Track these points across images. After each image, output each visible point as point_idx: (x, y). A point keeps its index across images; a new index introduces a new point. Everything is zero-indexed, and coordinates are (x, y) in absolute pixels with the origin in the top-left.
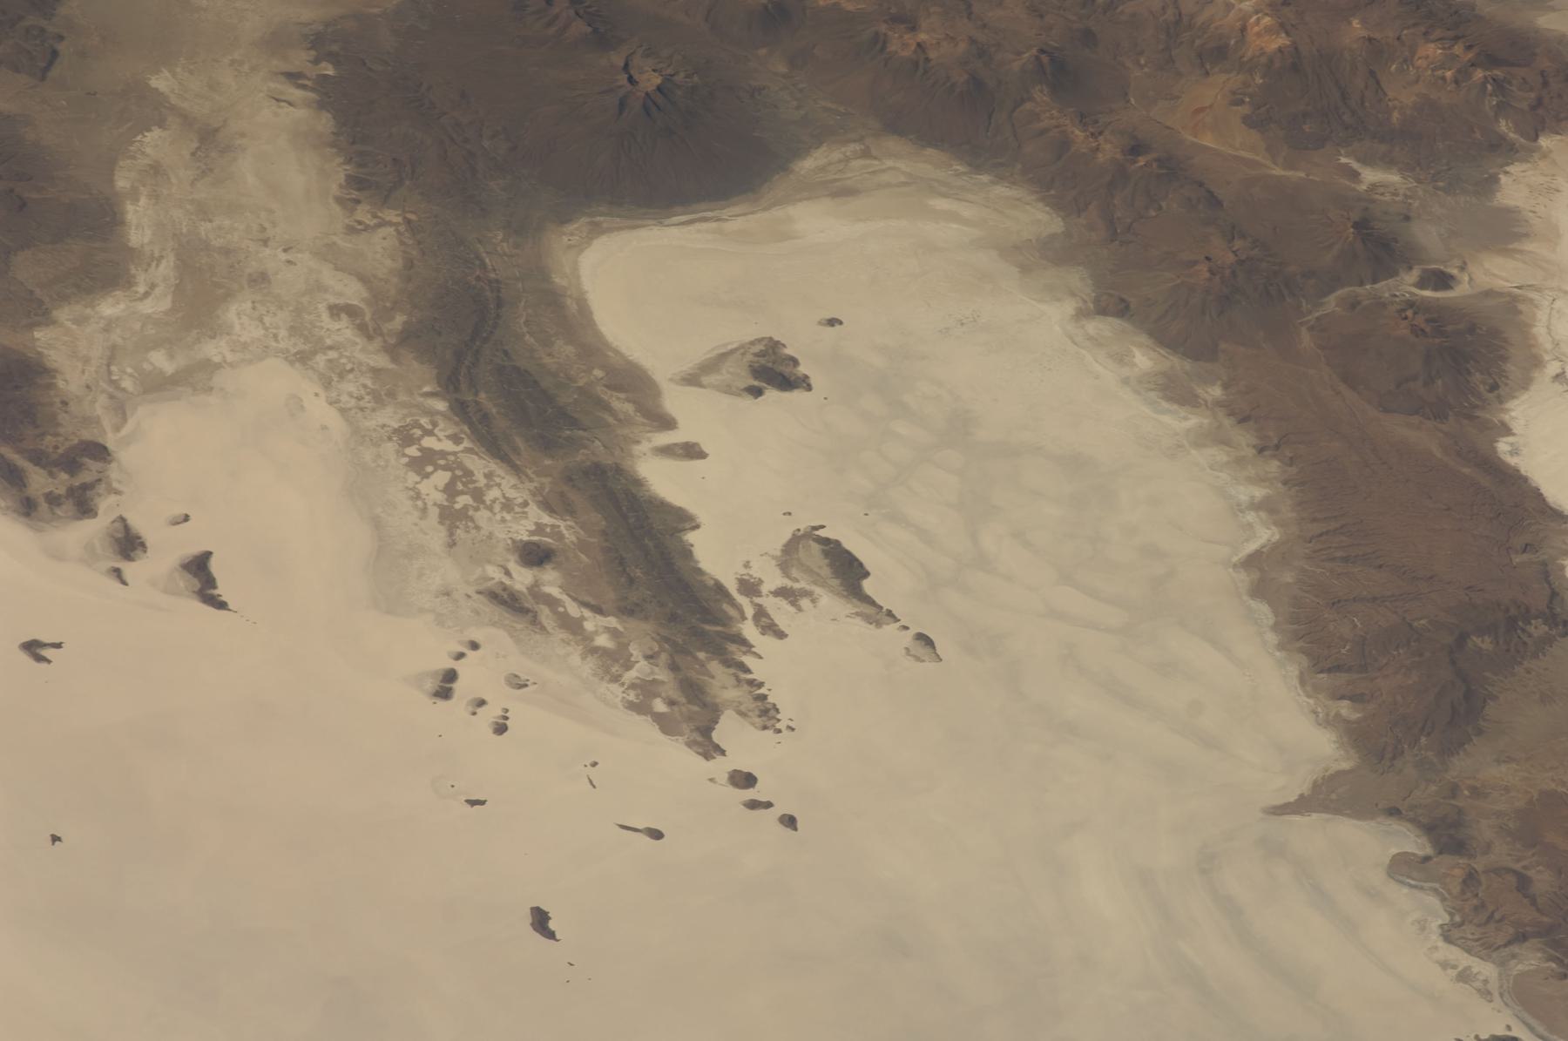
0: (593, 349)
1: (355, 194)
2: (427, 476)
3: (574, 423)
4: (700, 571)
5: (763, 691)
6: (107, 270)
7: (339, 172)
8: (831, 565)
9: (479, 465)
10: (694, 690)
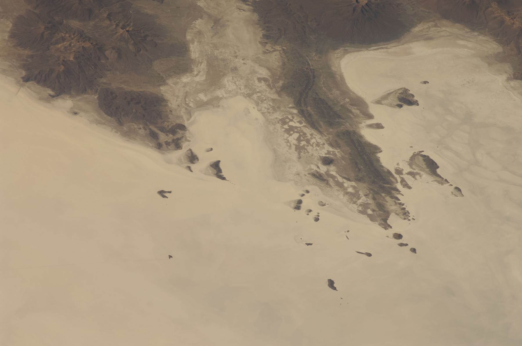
0: (346, 92)
1: (266, 41)
3: (340, 117)
4: (382, 166)
5: (404, 206)
6: (184, 67)
7: (260, 33)
8: (426, 164)
9: (308, 131)
10: (381, 207)
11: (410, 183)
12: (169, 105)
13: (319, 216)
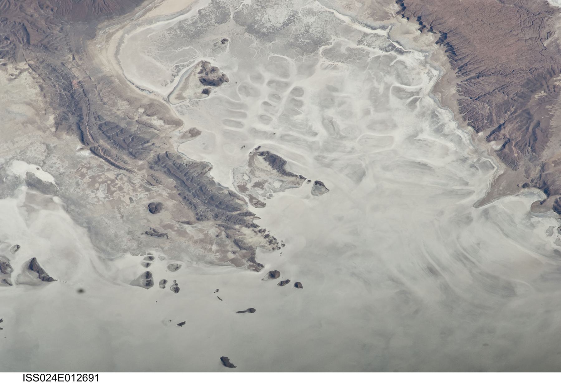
2: (98, 189)
4: (220, 187)
5: (266, 233)
11: (261, 199)
13: (176, 284)
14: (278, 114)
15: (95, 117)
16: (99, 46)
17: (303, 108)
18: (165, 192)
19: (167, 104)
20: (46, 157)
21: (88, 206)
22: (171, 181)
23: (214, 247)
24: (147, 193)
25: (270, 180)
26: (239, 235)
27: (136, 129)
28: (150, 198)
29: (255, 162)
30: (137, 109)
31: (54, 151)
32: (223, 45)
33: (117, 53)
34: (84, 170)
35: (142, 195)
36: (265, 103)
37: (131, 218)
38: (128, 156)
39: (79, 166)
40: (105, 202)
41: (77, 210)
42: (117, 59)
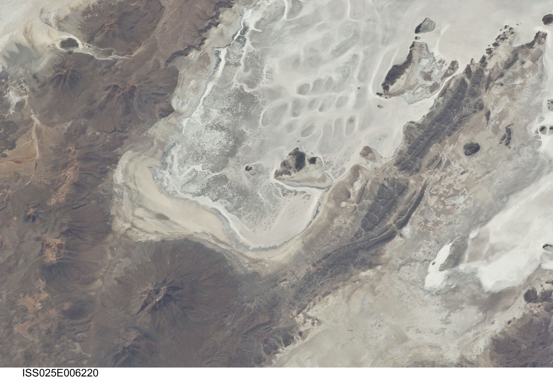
1: (296, 336)
2: (454, 205)
5: (492, 47)
11: (445, 68)
12: (499, 330)
14: (334, 94)
15: (357, 239)
16: (267, 265)
17: (323, 77)
18: (450, 149)
19: (333, 186)
20: (416, 261)
21: (478, 205)
22: (433, 150)
23: (518, 82)
24: (453, 163)
25: (420, 69)
26: (498, 67)
27: (368, 200)
28: (459, 157)
29: (397, 90)
30: (342, 208)
31: (408, 257)
32: (254, 168)
33: (275, 248)
34: (429, 225)
35: (456, 165)
36: (321, 110)
37: (489, 164)
38: (405, 195)
39: (425, 230)
40: (470, 193)
41: (485, 213)
42: (282, 245)
